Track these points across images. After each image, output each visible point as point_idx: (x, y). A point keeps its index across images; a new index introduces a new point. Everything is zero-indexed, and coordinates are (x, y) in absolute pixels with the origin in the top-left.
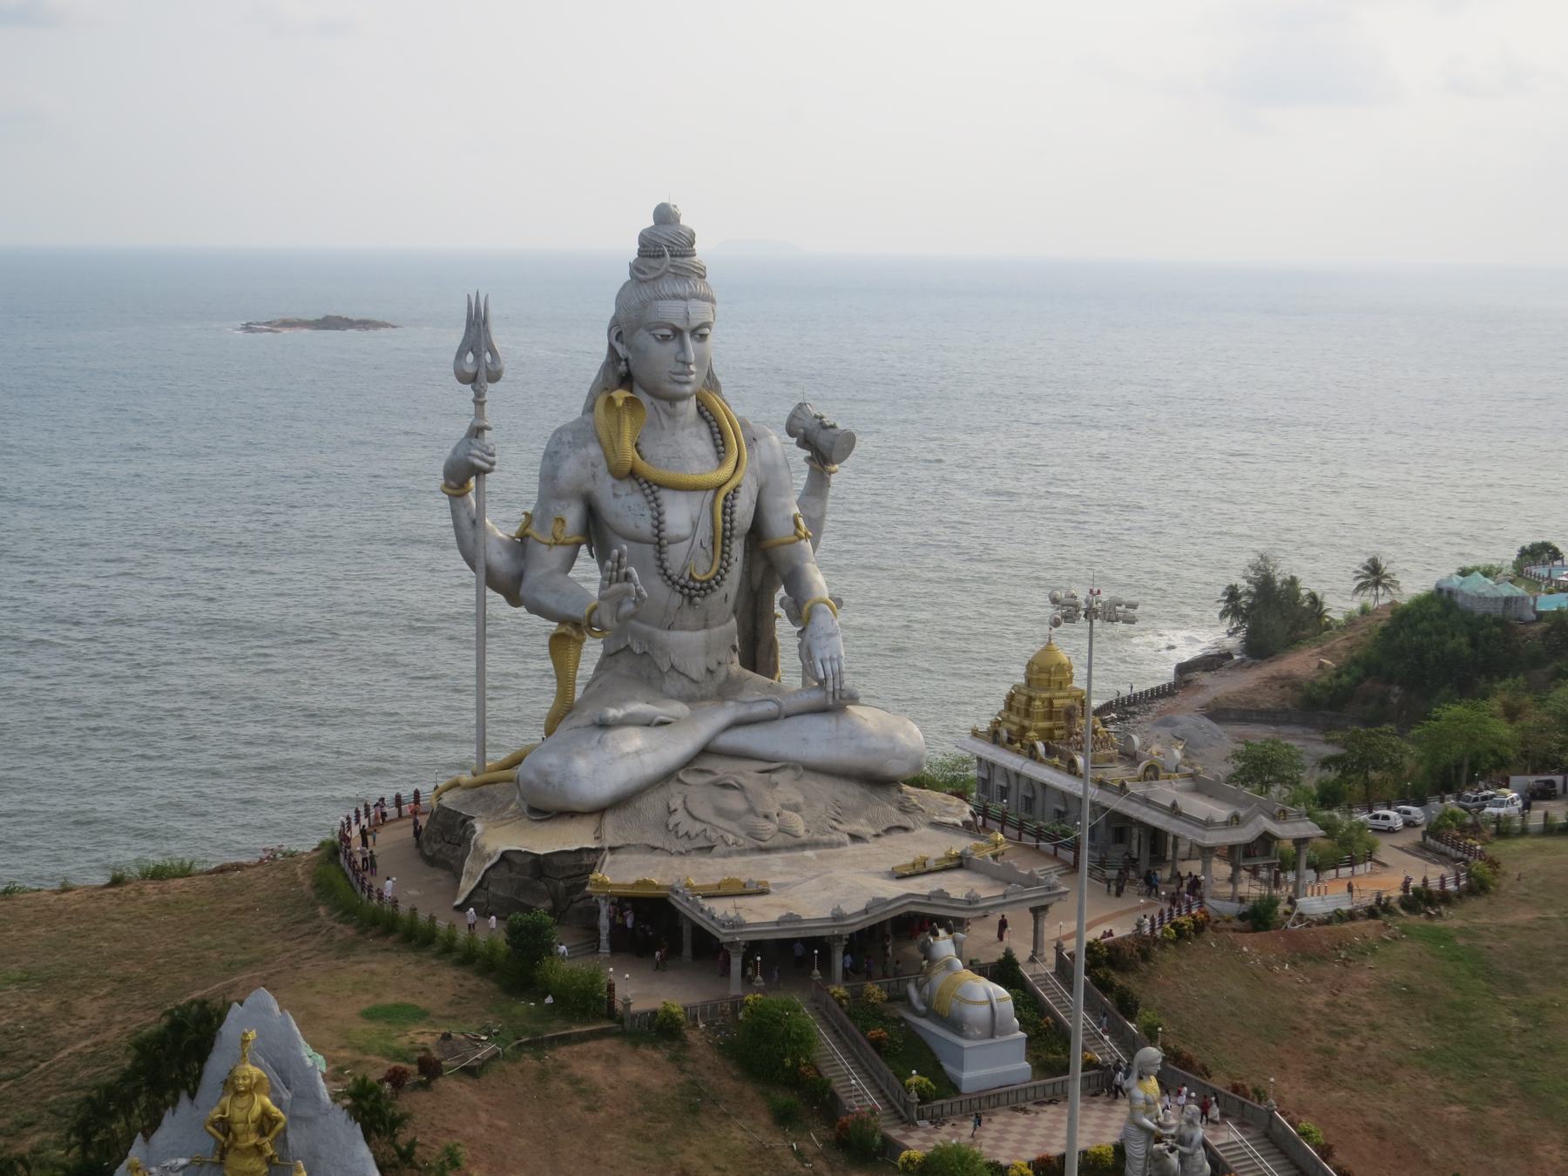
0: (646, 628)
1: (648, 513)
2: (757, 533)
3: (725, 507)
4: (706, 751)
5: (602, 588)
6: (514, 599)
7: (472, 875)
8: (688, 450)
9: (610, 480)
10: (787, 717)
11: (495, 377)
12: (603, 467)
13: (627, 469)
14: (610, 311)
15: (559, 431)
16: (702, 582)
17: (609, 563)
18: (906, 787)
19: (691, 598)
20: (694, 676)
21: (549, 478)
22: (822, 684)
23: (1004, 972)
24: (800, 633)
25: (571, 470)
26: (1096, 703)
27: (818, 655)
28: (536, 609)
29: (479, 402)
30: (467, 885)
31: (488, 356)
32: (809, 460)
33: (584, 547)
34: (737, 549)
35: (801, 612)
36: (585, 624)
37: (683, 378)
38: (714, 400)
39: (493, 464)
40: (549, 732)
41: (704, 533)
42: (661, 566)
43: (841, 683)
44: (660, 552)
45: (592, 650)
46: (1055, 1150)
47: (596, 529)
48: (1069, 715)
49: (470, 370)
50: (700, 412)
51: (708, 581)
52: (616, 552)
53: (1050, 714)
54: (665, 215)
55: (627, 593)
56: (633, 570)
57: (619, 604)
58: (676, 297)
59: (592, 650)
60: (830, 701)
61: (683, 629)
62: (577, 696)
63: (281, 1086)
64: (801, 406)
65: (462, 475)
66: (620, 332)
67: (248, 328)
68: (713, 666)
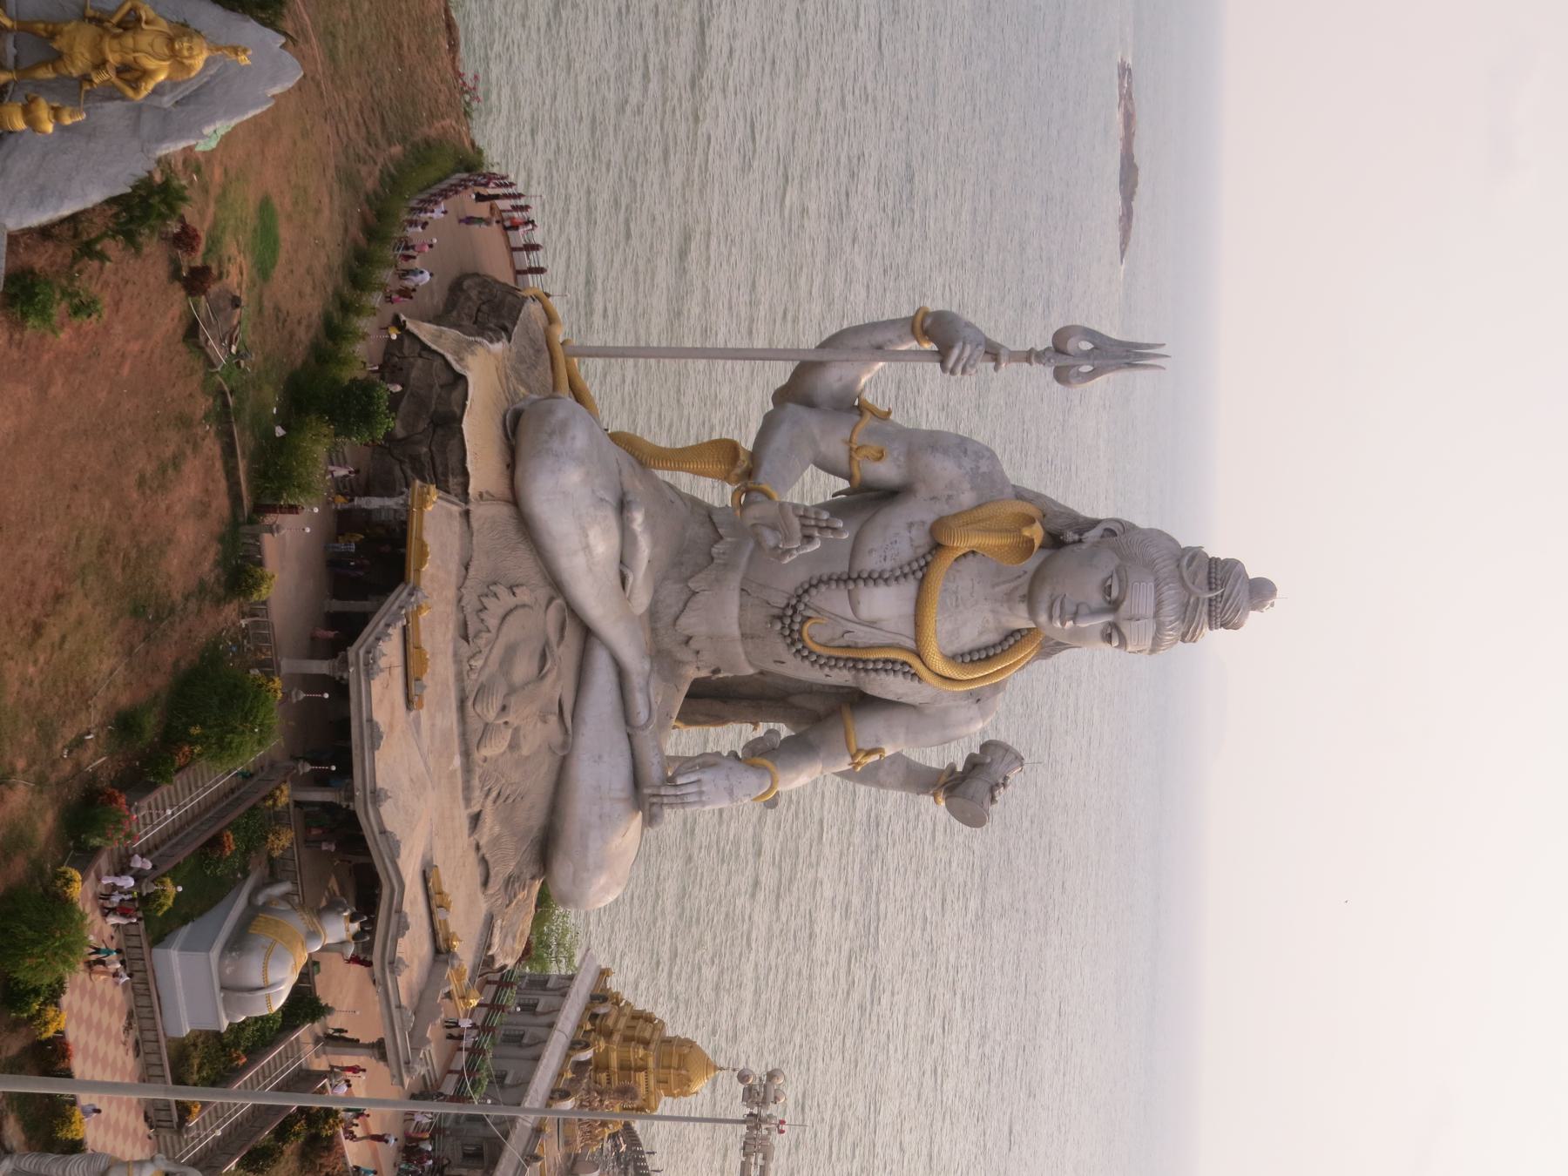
0: (744, 561)
1: (888, 565)
2: (860, 701)
3: (894, 662)
4: (588, 633)
5: (795, 507)
6: (782, 396)
7: (438, 337)
8: (965, 617)
9: (930, 518)
10: (629, 736)
11: (1061, 376)
12: (944, 509)
13: (944, 540)
14: (1142, 522)
15: (993, 456)
16: (800, 632)
17: (825, 515)
18: (537, 884)
19: (781, 618)
20: (683, 621)
21: (934, 442)
22: (670, 781)
23: (304, 1004)
24: (734, 755)
25: (944, 469)
26: (637, 1125)
27: (706, 776)
28: (769, 424)
29: (1030, 356)
30: (425, 331)
31: (1086, 368)
32: (952, 768)
33: (843, 484)
34: (841, 677)
35: (759, 755)
36: (750, 485)
37: (1057, 612)
38: (1029, 650)
39: (952, 372)
40: (616, 438)
41: (863, 635)
42: (820, 581)
43: (671, 805)
44: (838, 580)
45: (715, 492)
46: (78, 1065)
47: (870, 498)
48: (625, 1092)
49: (1071, 346)
50: (1013, 633)
51: (801, 640)
52: (840, 524)
53: (625, 1067)
54: (1261, 592)
55: (787, 539)
56: (817, 545)
57: (774, 528)
58: (1159, 604)
59: (715, 492)
60: (647, 791)
61: (742, 607)
62: (660, 474)
63: (179, 94)
64: (1019, 759)
65: (939, 334)
66: (1115, 533)
67: (1125, 71)
68: (694, 645)
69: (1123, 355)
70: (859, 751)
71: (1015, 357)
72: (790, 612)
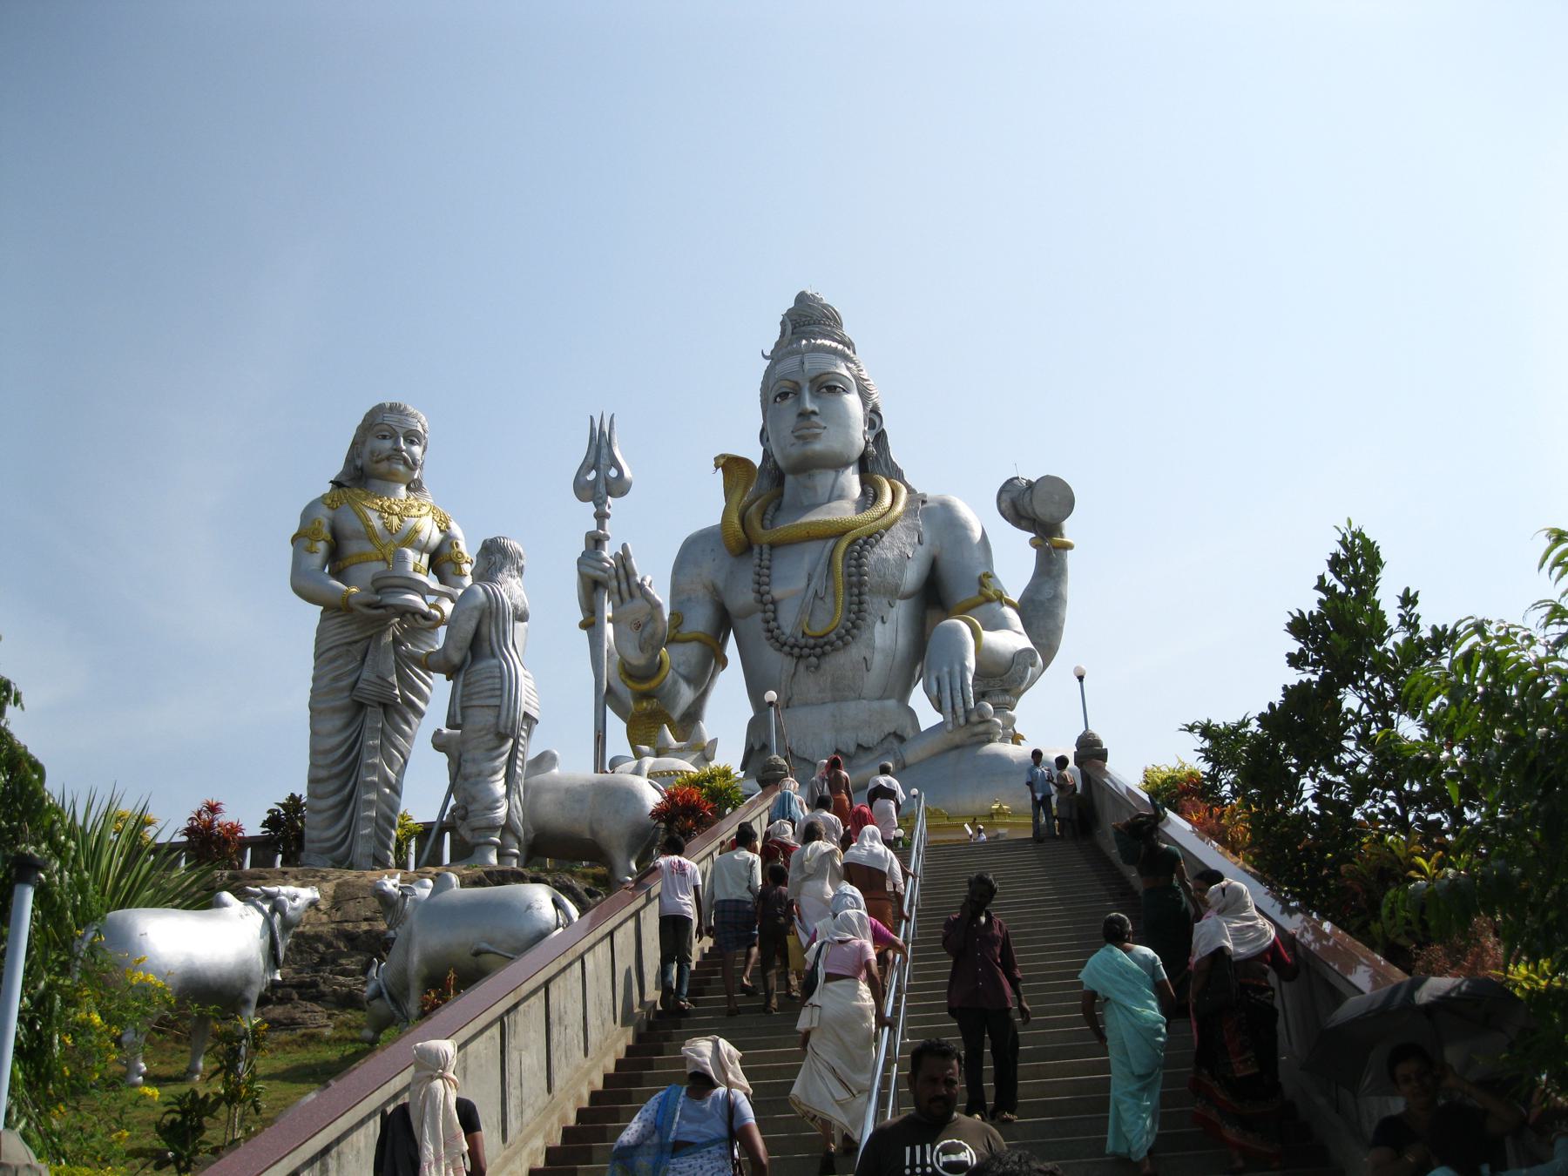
11: (619, 487)
29: (601, 517)
69: (600, 450)
70: (980, 593)
71: (601, 525)
72: (796, 650)
